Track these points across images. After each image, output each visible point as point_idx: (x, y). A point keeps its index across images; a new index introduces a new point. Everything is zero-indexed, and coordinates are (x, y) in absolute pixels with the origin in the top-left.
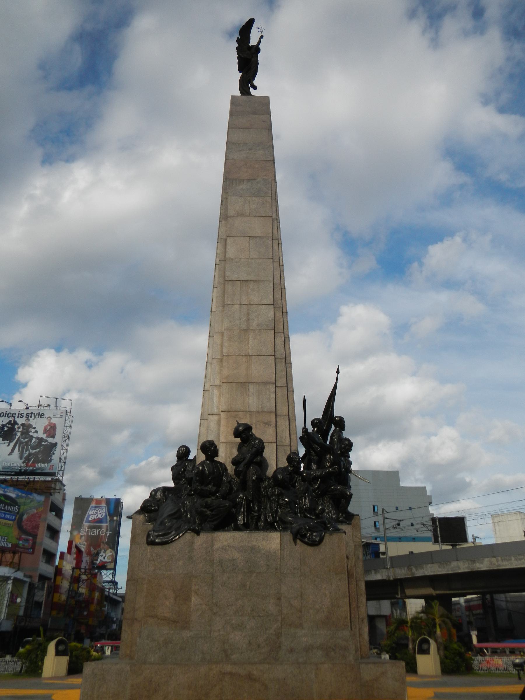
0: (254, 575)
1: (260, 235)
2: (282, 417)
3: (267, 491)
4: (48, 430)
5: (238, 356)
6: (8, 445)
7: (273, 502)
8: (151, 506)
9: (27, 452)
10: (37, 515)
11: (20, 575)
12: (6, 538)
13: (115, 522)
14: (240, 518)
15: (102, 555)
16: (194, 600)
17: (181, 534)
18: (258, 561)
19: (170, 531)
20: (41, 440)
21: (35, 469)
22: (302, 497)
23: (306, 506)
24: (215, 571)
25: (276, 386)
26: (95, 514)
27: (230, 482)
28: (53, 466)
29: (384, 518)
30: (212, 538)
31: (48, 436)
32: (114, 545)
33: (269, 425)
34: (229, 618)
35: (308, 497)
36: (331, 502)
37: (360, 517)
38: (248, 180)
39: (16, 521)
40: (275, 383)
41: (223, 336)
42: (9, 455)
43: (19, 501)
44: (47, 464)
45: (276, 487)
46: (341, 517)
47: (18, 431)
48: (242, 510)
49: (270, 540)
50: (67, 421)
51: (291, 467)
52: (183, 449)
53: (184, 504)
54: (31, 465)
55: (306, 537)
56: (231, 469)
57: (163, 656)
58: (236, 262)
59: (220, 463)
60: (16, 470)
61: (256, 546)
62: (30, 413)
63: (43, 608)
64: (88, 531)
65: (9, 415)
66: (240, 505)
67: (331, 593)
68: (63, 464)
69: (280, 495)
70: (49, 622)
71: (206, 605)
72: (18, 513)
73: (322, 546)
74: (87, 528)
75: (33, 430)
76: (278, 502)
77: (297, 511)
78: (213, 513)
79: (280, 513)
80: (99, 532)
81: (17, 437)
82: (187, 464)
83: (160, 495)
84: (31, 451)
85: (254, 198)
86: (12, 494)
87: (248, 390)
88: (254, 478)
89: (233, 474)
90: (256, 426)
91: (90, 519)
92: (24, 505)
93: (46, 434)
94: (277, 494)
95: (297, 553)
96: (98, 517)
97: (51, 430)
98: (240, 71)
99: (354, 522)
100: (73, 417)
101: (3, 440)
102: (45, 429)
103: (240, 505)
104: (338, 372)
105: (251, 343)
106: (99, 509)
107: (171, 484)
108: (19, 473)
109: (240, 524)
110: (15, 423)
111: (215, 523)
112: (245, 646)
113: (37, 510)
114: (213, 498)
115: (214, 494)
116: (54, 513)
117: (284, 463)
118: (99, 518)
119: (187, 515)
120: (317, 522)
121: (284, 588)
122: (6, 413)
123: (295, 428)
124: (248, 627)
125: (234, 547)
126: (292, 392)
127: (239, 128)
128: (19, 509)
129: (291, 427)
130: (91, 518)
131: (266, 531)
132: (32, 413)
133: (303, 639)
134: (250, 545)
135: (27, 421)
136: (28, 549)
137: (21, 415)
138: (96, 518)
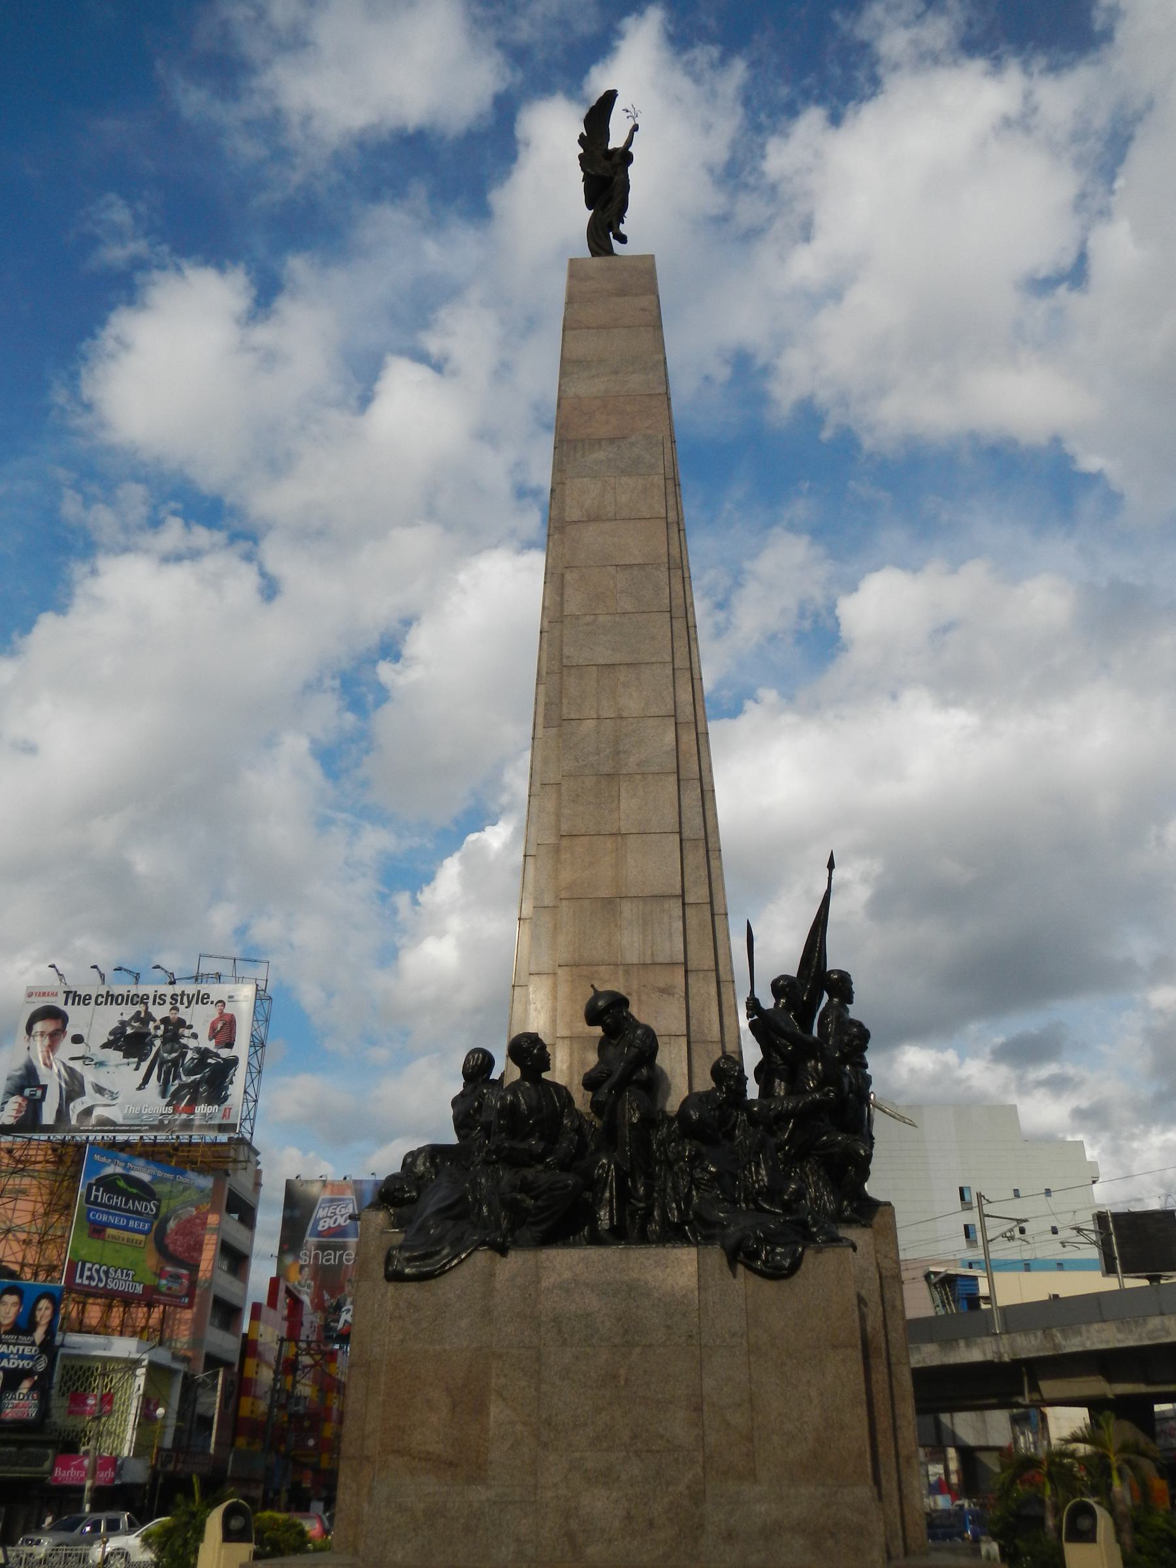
0: (638, 1350)
1: (639, 560)
2: (701, 975)
3: (665, 1149)
4: (219, 1032)
5: (596, 837)
7: (680, 1174)
8: (402, 1189)
10: (198, 1221)
11: (163, 1356)
14: (603, 1214)
15: (348, 1310)
16: (496, 1411)
17: (463, 1256)
18: (646, 1318)
19: (438, 1248)
20: (204, 1054)
22: (750, 1163)
23: (761, 1183)
24: (543, 1342)
25: (684, 904)
26: (331, 1217)
27: (579, 1130)
28: (230, 1109)
29: (983, 1216)
30: (537, 1262)
31: (218, 1045)
33: (669, 994)
34: (578, 1455)
35: (766, 1163)
36: (822, 1173)
37: (893, 1208)
38: (612, 441)
39: (152, 1235)
40: (683, 896)
41: (559, 791)
43: (158, 1188)
44: (219, 1106)
45: (686, 1141)
46: (846, 1210)
47: (156, 1036)
48: (607, 1195)
49: (672, 1267)
51: (721, 1091)
52: (476, 1057)
53: (475, 1184)
54: (183, 1109)
55: (759, 1257)
56: (581, 1099)
57: (423, 1546)
58: (587, 624)
59: (555, 1085)
61: (639, 1280)
62: (179, 993)
63: (214, 1432)
65: (136, 999)
66: (602, 1183)
67: (822, 1394)
68: (251, 1104)
69: (696, 1158)
70: (230, 1463)
71: (525, 1424)
72: (156, 1216)
73: (797, 1279)
74: (313, 1248)
75: (187, 1032)
76: (691, 1175)
77: (739, 1196)
78: (540, 1203)
79: (696, 1200)
82: (485, 1091)
83: (424, 1164)
84: (184, 1078)
85: (624, 479)
87: (618, 913)
88: (635, 1120)
89: (589, 1110)
90: (639, 996)
91: (320, 1228)
92: (169, 1199)
93: (214, 1040)
94: (688, 1157)
95: (738, 1296)
96: (337, 1224)
98: (589, 207)
99: (877, 1220)
102: (213, 1028)
103: (602, 1183)
104: (831, 865)
105: (623, 804)
106: (338, 1206)
107: (452, 1139)
109: (602, 1230)
110: (149, 1017)
111: (544, 1227)
112: (617, 1523)
113: (197, 1208)
114: (540, 1167)
115: (540, 1159)
116: (236, 1216)
117: (704, 1083)
118: (339, 1225)
119: (481, 1209)
120: (785, 1222)
121: (709, 1383)
122: (128, 996)
123: (732, 999)
124: (624, 1477)
125: (587, 1285)
126: (724, 916)
127: (589, 328)
128: (158, 1208)
129: (724, 997)
130: (323, 1227)
131: (664, 1246)
132: (183, 994)
133: (758, 1506)
134: (627, 1278)
135: (173, 1011)
136: (180, 1297)
137: (160, 998)
138: (332, 1226)
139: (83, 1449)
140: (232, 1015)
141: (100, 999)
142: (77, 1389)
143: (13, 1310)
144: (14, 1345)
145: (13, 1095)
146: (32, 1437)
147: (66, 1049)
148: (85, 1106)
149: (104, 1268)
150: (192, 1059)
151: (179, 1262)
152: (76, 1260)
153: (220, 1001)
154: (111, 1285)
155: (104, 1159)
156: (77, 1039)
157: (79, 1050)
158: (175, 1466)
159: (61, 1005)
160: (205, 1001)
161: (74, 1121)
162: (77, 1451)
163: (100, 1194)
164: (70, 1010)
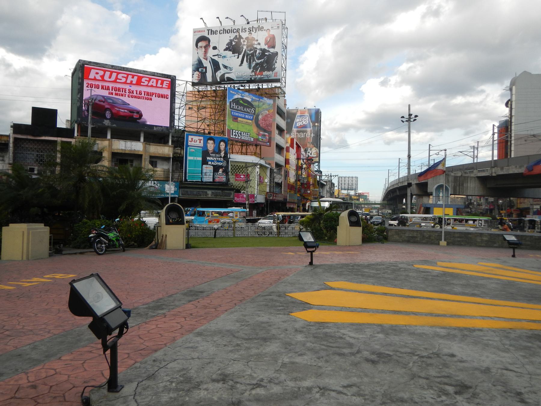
4: (268, 42)
6: (238, 58)
9: (254, 62)
10: (269, 116)
11: (262, 162)
12: (249, 134)
13: (317, 127)
20: (264, 51)
21: (262, 76)
26: (301, 122)
28: (277, 73)
31: (269, 47)
32: (317, 144)
42: (240, 66)
43: (254, 103)
47: (245, 45)
50: (284, 32)
60: (248, 78)
62: (251, 27)
63: (283, 187)
64: (297, 134)
65: (235, 31)
72: (254, 114)
75: (256, 43)
80: (305, 134)
81: (244, 50)
84: (257, 61)
86: (248, 98)
91: (297, 125)
97: (271, 42)
100: (287, 28)
101: (233, 54)
102: (266, 40)
108: (250, 81)
110: (240, 37)
122: (232, 30)
128: (255, 111)
136: (266, 143)
137: (244, 29)
139: (242, 192)
140: (274, 35)
141: (221, 32)
142: (237, 172)
143: (212, 146)
144: (215, 157)
145: (196, 71)
146: (225, 188)
147: (211, 53)
148: (221, 74)
149: (239, 132)
150: (259, 53)
151: (265, 131)
152: (230, 129)
153: (268, 29)
154: (243, 138)
155: (234, 93)
156: (215, 48)
157: (216, 52)
158: (273, 197)
159: (207, 36)
160: (262, 30)
161: (219, 80)
162: (240, 192)
163: (234, 105)
164: (211, 37)
